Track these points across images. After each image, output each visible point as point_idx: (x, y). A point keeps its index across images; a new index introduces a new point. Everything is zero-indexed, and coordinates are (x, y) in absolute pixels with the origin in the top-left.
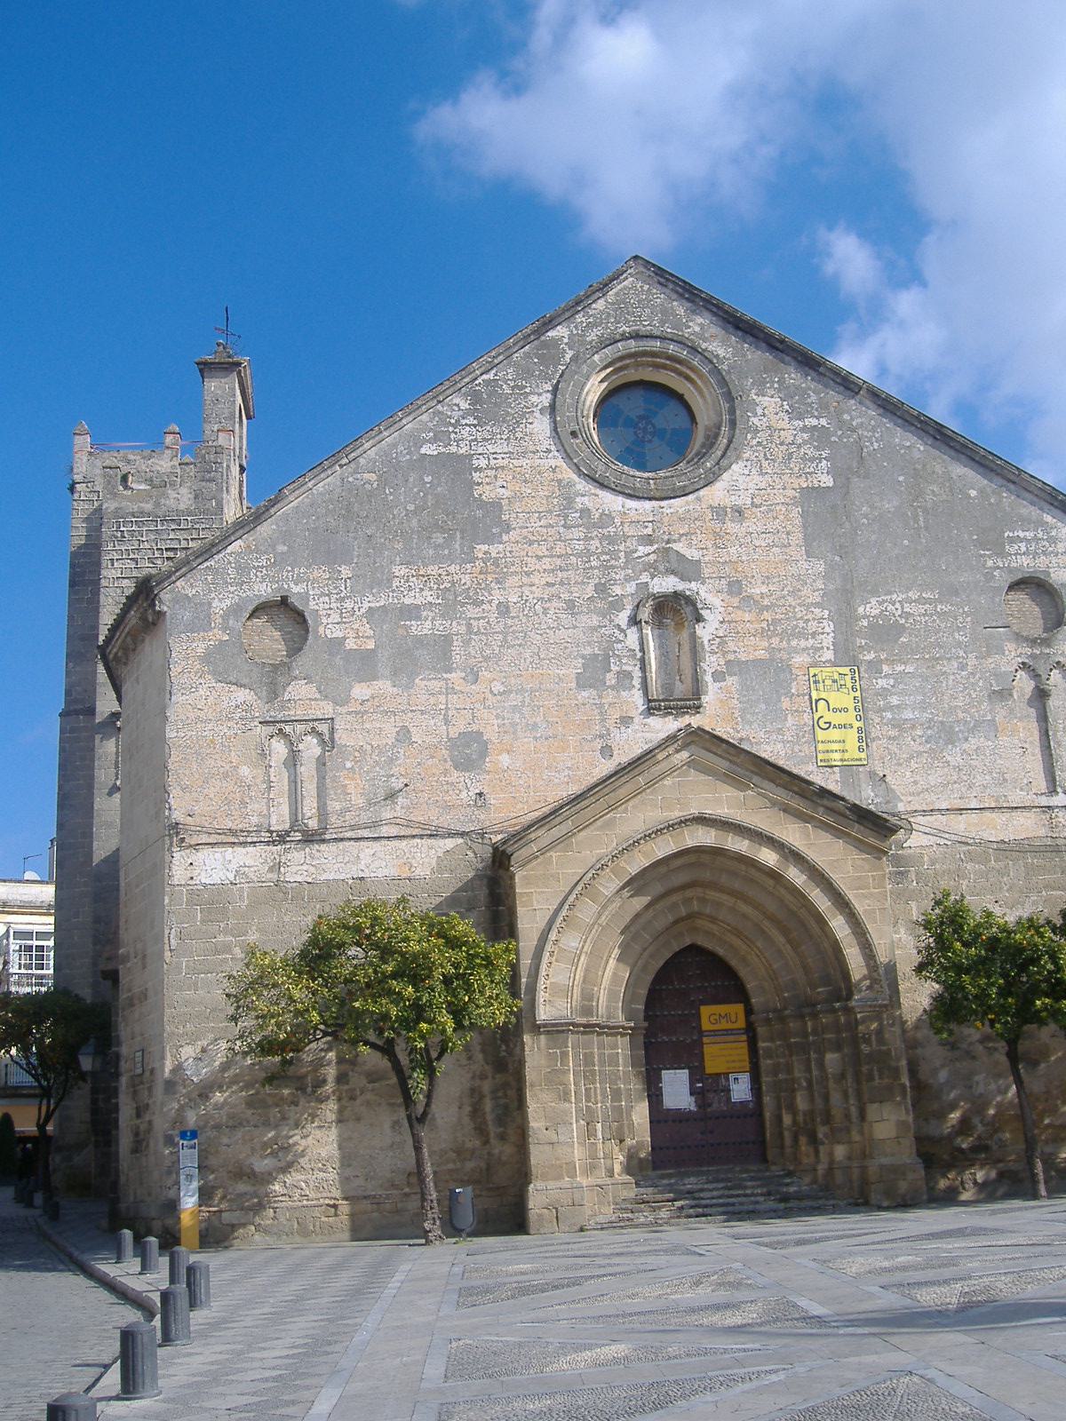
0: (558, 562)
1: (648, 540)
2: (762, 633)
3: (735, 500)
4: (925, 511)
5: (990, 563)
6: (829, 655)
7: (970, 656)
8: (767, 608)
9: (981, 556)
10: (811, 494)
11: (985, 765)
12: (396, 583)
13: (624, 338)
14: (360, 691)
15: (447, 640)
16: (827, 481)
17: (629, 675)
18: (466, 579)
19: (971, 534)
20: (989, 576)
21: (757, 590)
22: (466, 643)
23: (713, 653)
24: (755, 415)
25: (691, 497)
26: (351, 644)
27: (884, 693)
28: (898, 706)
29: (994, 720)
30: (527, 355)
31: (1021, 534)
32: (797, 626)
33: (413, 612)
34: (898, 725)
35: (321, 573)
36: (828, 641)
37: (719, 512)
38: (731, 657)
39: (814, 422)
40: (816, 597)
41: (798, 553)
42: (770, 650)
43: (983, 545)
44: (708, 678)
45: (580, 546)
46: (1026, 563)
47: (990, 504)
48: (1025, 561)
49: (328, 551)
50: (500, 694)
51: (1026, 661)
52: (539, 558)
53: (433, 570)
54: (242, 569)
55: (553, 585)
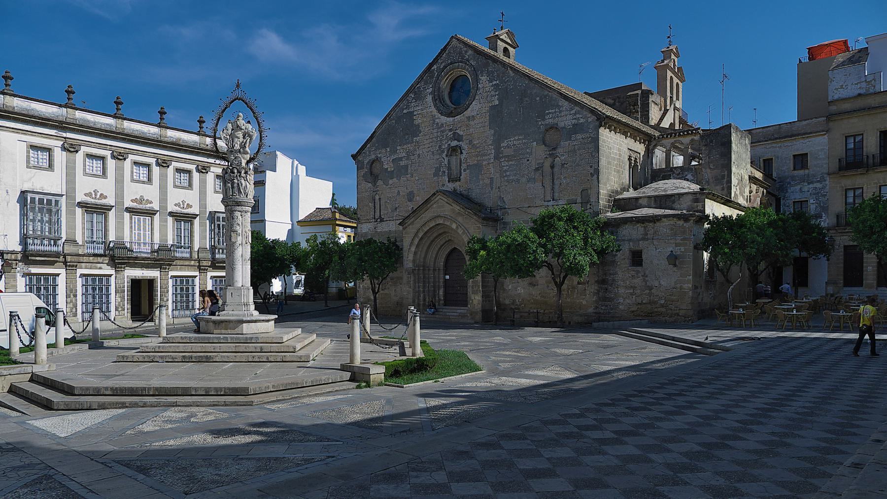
0: (431, 140)
1: (450, 130)
2: (477, 156)
3: (475, 113)
4: (523, 107)
5: (540, 123)
8: (478, 148)
10: (493, 108)
13: (449, 65)
14: (391, 182)
16: (497, 103)
17: (444, 172)
22: (411, 166)
23: (464, 163)
24: (480, 84)
25: (462, 115)
26: (389, 170)
28: (509, 175)
29: (535, 178)
30: (427, 77)
31: (551, 111)
32: (485, 152)
33: (401, 159)
34: (508, 181)
35: (384, 151)
37: (468, 118)
38: (468, 164)
39: (495, 82)
41: (487, 128)
42: (477, 160)
44: (462, 171)
45: (435, 134)
47: (543, 102)
48: (551, 121)
49: (385, 146)
50: (418, 180)
53: (405, 147)
54: (370, 153)
55: (429, 147)
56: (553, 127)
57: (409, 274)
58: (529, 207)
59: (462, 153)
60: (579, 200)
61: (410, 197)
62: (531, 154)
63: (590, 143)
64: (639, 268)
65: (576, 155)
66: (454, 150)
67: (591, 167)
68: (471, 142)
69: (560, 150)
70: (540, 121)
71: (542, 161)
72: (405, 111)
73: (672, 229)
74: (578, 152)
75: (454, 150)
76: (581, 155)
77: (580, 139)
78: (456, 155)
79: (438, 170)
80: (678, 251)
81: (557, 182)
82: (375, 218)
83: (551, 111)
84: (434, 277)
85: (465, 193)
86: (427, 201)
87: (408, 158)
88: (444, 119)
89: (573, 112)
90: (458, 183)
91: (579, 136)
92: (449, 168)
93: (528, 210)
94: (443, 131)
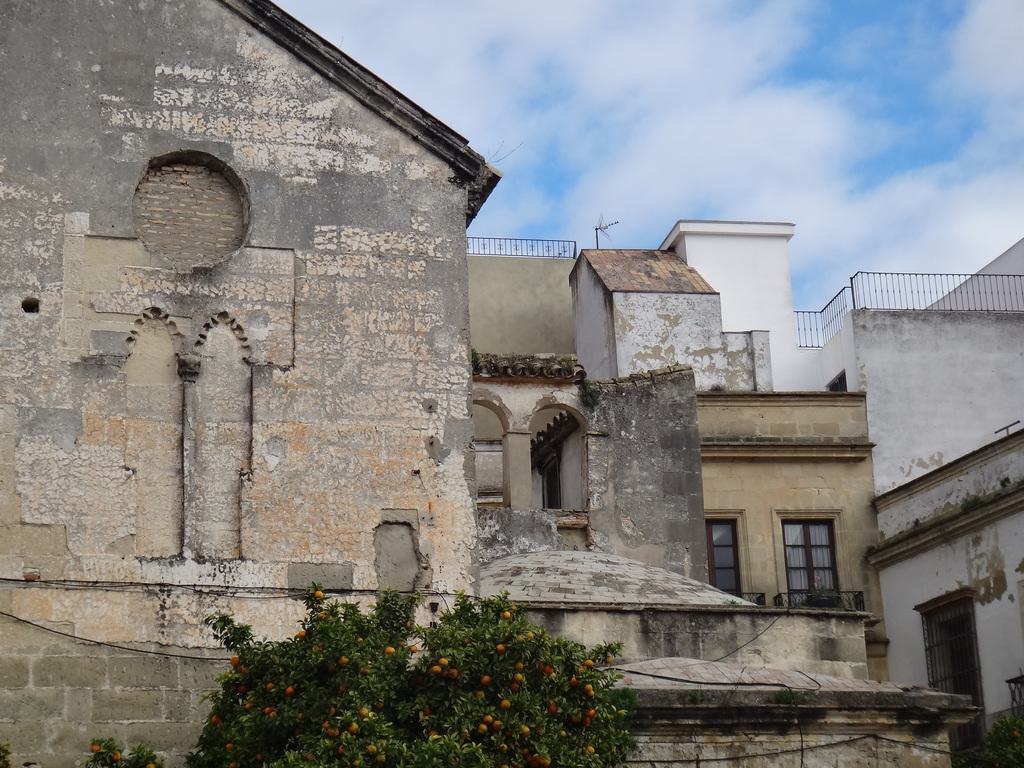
5: (117, 119)
7: (48, 285)
9: (103, 104)
11: (45, 496)
19: (90, 62)
20: (112, 142)
31: (187, 72)
43: (105, 81)
46: (186, 127)
47: (137, 12)
48: (187, 122)
51: (161, 305)
58: (29, 580)
62: (51, 270)
63: (425, 283)
65: (342, 331)
67: (430, 407)
70: (119, 107)
71: (127, 326)
74: (354, 319)
76: (367, 334)
77: (358, 252)
83: (187, 72)
91: (358, 239)
93: (27, 602)
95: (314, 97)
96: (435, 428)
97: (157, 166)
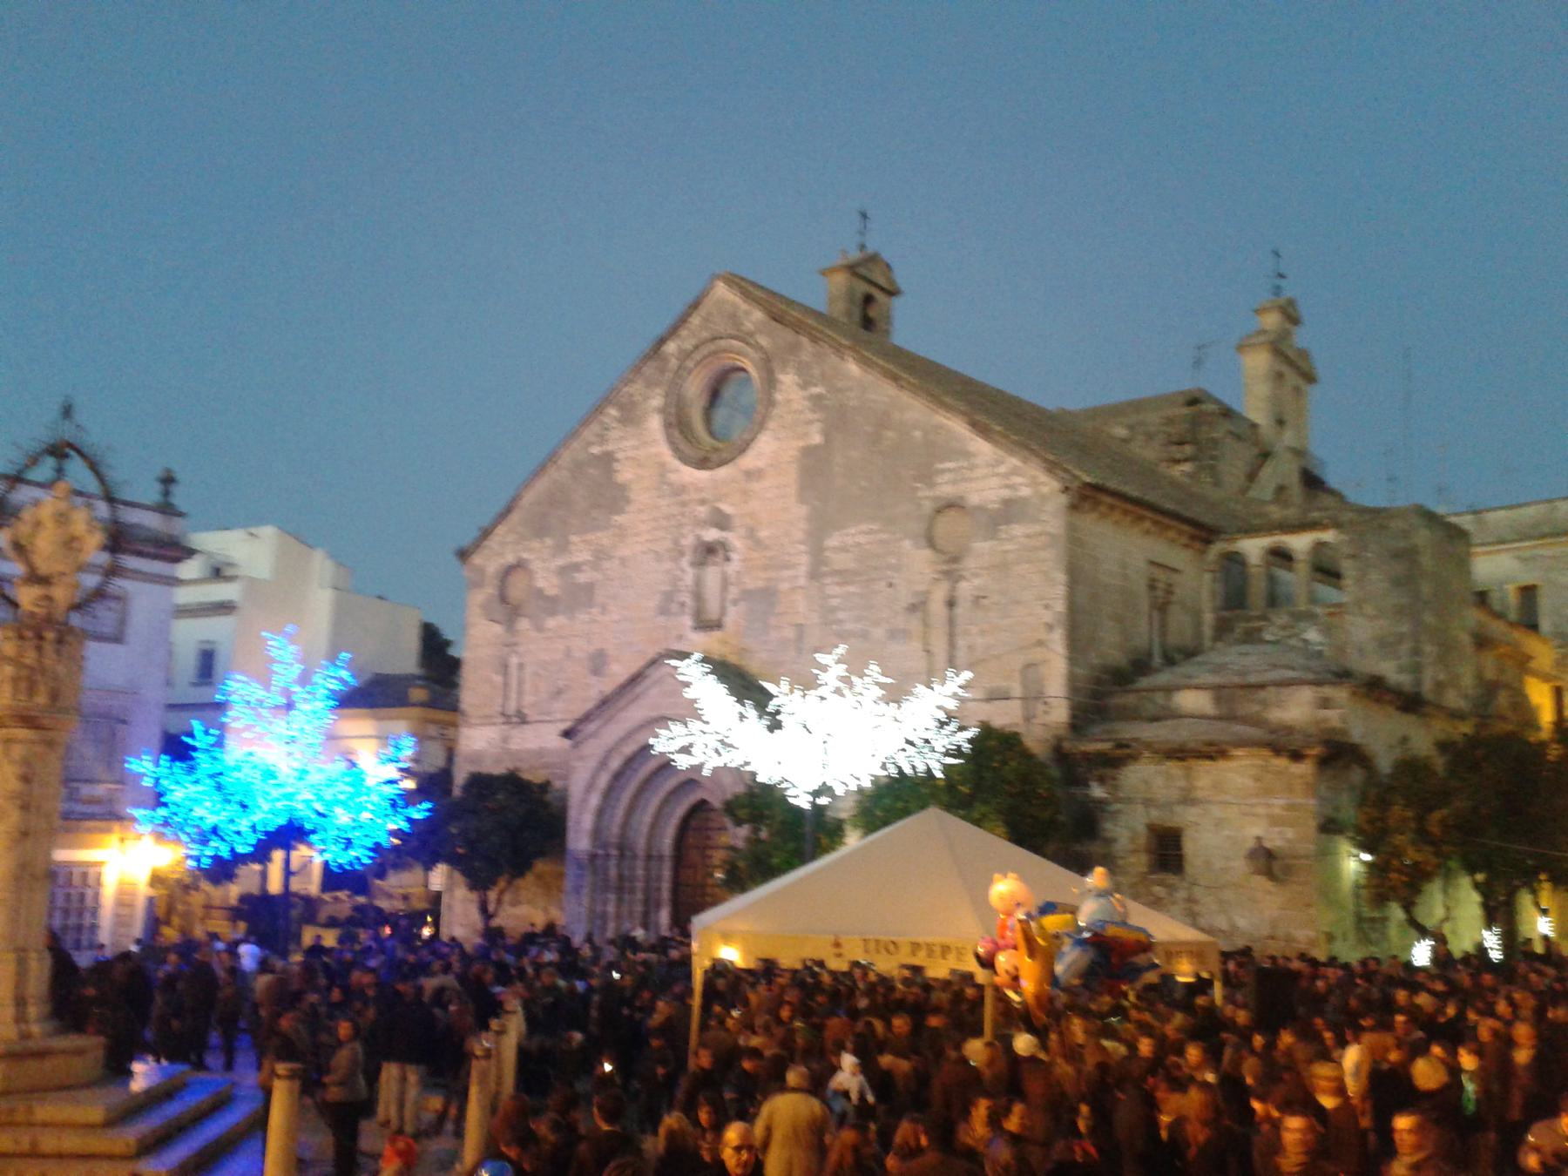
1: (703, 502)
2: (766, 568)
3: (760, 464)
6: (802, 582)
10: (808, 452)
12: (573, 548)
14: (551, 623)
15: (590, 588)
16: (817, 439)
17: (683, 604)
18: (605, 541)
21: (763, 534)
27: (833, 610)
33: (577, 567)
35: (536, 544)
36: (803, 570)
37: (750, 475)
40: (799, 535)
44: (728, 604)
49: (540, 531)
52: (643, 522)
53: (590, 537)
56: (952, 505)
57: (580, 866)
59: (728, 559)
60: (1017, 690)
61: (598, 664)
64: (1171, 879)
66: (709, 551)
67: (1047, 607)
68: (751, 534)
69: (970, 563)
72: (595, 450)
73: (1257, 779)
75: (709, 551)
78: (715, 564)
79: (669, 597)
80: (1276, 839)
81: (961, 642)
82: (503, 714)
84: (648, 879)
85: (733, 659)
86: (635, 679)
87: (596, 564)
88: (689, 474)
89: (1002, 469)
90: (717, 634)
91: (1018, 530)
92: (698, 596)
94: (684, 504)
95: (999, 462)
96: (1048, 617)
97: (939, 511)
